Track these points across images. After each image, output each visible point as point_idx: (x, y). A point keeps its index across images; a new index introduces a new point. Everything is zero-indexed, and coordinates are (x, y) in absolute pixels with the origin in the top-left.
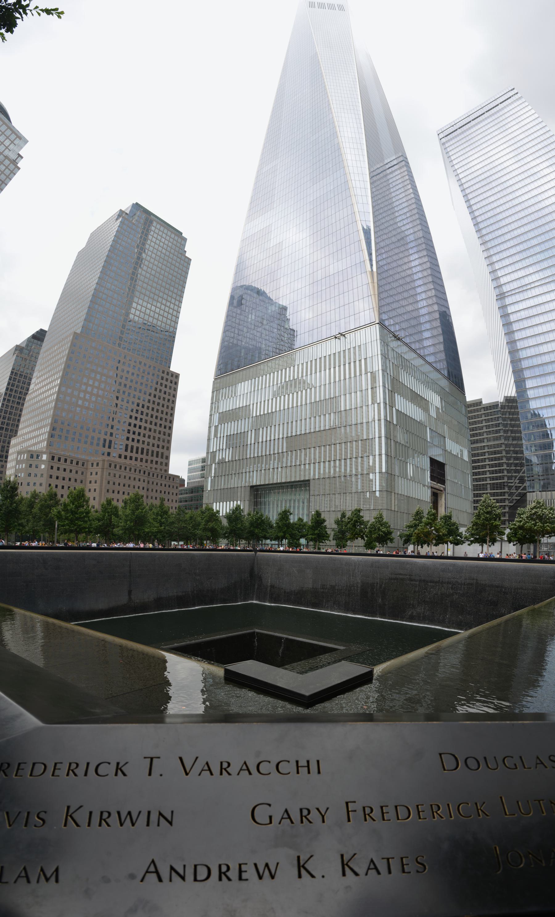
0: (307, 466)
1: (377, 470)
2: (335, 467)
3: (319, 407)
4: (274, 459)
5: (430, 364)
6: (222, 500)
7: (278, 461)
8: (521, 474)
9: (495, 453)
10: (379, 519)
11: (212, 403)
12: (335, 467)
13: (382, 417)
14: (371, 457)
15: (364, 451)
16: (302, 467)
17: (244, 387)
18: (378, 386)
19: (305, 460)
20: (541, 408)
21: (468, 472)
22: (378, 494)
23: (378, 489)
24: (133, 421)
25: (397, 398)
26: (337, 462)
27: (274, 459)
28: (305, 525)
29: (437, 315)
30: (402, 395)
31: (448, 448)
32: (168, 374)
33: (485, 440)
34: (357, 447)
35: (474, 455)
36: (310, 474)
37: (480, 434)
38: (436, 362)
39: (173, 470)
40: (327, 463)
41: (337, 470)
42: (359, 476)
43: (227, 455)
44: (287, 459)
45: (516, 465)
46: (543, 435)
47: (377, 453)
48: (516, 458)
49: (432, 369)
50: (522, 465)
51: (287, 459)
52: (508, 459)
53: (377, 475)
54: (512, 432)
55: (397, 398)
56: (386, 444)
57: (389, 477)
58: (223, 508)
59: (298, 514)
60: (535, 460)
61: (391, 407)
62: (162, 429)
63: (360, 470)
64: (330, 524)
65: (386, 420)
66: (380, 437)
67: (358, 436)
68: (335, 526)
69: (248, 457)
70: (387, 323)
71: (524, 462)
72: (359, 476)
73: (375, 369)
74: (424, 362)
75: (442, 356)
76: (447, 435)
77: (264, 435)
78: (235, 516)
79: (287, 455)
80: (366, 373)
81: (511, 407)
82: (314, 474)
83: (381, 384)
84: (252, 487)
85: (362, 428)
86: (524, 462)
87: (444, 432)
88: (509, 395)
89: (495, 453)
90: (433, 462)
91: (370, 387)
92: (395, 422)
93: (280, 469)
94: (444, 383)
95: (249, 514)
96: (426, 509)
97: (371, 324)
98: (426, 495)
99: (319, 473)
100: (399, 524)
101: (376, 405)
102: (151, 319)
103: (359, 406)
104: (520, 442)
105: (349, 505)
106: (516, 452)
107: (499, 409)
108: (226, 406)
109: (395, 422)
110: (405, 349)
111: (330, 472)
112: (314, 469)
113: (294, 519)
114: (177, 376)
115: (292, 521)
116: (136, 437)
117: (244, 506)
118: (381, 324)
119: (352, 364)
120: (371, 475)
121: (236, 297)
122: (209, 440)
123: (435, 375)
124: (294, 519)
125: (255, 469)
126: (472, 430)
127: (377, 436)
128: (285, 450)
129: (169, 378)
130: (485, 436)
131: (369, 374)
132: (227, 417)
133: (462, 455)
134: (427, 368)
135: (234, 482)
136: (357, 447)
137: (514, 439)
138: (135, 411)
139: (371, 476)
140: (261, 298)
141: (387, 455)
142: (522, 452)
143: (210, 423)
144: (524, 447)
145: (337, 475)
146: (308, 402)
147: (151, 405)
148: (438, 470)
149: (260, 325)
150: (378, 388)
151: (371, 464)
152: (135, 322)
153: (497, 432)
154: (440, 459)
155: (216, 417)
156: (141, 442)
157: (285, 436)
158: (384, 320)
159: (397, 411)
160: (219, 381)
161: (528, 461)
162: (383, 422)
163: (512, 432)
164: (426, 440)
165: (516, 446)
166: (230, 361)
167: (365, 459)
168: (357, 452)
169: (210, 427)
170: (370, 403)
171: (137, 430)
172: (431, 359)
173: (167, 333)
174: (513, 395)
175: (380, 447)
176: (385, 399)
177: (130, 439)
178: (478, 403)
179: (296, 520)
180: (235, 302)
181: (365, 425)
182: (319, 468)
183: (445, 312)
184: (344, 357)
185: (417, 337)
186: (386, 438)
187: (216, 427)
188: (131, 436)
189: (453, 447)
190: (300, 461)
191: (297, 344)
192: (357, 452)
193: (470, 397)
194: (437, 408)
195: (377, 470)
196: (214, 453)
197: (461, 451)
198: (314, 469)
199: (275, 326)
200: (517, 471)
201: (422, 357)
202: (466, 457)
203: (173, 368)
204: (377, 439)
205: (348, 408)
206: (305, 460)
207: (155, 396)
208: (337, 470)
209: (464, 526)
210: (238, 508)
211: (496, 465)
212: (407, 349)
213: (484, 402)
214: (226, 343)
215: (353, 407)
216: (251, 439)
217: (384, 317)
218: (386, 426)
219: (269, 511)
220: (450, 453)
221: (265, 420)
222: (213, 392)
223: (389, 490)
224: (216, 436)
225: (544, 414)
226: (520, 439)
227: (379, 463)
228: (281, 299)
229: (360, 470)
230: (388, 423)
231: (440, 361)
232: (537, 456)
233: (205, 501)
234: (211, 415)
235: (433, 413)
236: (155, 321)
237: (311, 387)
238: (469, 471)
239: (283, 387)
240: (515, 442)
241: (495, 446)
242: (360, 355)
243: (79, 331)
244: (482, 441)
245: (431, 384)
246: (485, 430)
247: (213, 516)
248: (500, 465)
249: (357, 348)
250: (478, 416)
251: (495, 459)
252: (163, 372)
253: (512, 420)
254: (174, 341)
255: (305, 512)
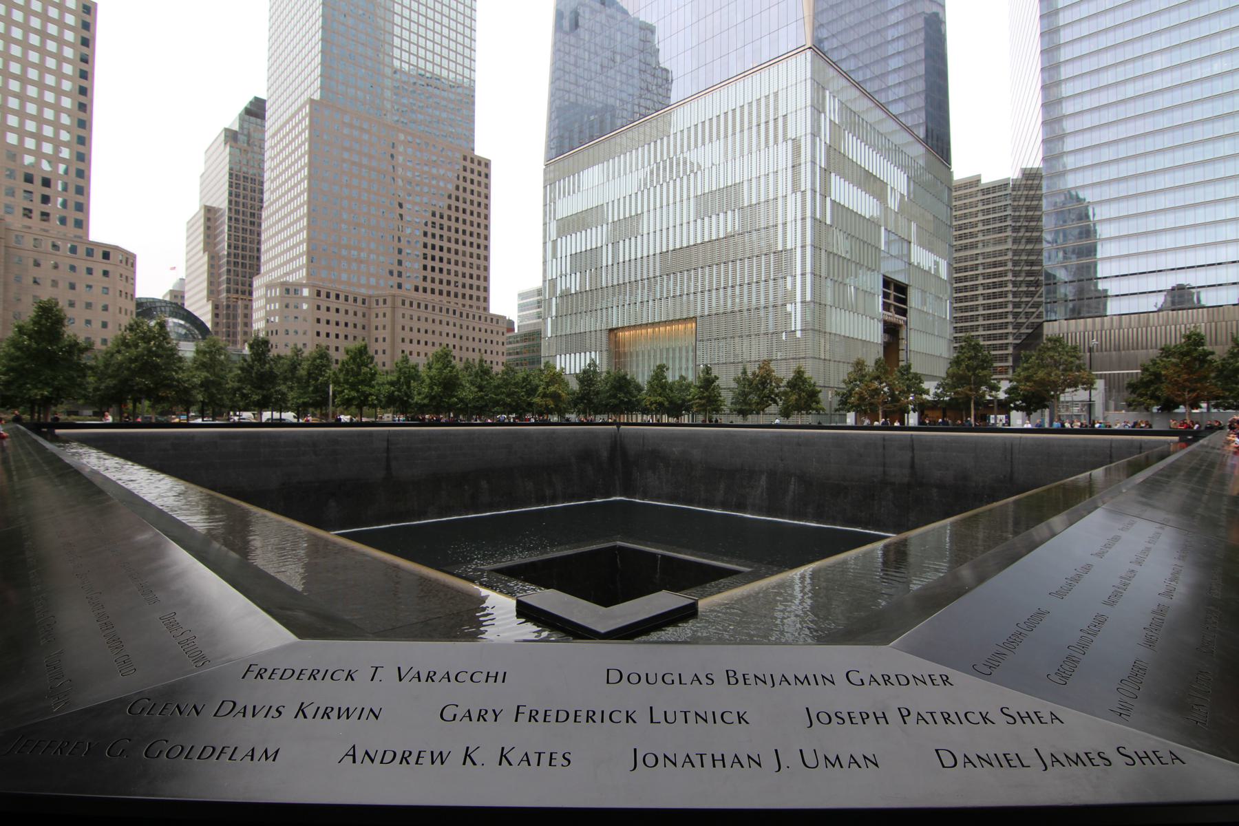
0: (692, 296)
1: (798, 299)
2: (733, 296)
3: (709, 204)
4: (643, 288)
5: (895, 118)
6: (568, 351)
7: (649, 291)
8: (1036, 299)
9: (995, 265)
10: (799, 374)
11: (545, 205)
12: (733, 296)
13: (808, 214)
14: (789, 279)
15: (778, 269)
16: (685, 297)
17: (592, 176)
18: (803, 161)
19: (688, 287)
20: (1083, 187)
21: (946, 297)
22: (798, 334)
23: (799, 327)
24: (430, 241)
25: (835, 180)
26: (737, 288)
27: (643, 288)
28: (689, 386)
29: (920, 23)
30: (843, 175)
31: (914, 259)
32: (472, 161)
33: (980, 245)
34: (768, 264)
35: (958, 270)
36: (696, 310)
37: (972, 235)
38: (905, 114)
39: (495, 308)
40: (721, 291)
41: (737, 300)
42: (771, 309)
43: (573, 284)
44: (662, 285)
45: (1029, 284)
46: (1081, 233)
47: (799, 272)
48: (1029, 273)
49: (898, 127)
50: (1037, 284)
51: (662, 285)
52: (1016, 274)
53: (799, 305)
54: (1028, 229)
55: (835, 180)
56: (813, 256)
57: (817, 306)
58: (571, 364)
59: (680, 368)
60: (1062, 275)
61: (824, 196)
62: (475, 250)
63: (771, 299)
64: (726, 381)
65: (814, 218)
66: (803, 247)
67: (769, 246)
68: (733, 385)
69: (604, 285)
70: (826, 46)
71: (1042, 278)
72: (771, 309)
73: (801, 132)
74: (884, 116)
75: (920, 102)
76: (913, 239)
77: (627, 251)
78: (587, 377)
79: (662, 280)
80: (785, 140)
81: (1031, 188)
82: (703, 308)
83: (809, 159)
84: (611, 330)
85: (776, 232)
86: (1042, 278)
87: (909, 235)
88: (1029, 166)
89: (995, 265)
90: (887, 282)
91: (790, 165)
92: (828, 222)
93: (651, 303)
94: (918, 151)
95: (608, 373)
96: (873, 356)
97: (798, 51)
98: (876, 334)
99: (710, 307)
100: (830, 379)
101: (799, 194)
102: (429, 67)
103: (771, 197)
104: (1037, 247)
105: (752, 353)
106: (1032, 263)
107: (1009, 191)
108: (568, 207)
109: (828, 222)
110: (855, 93)
111: (725, 304)
112: (703, 301)
113: (674, 376)
114: (487, 164)
115: (670, 380)
116: (437, 264)
117: (601, 359)
118: (817, 49)
119: (763, 126)
120: (789, 306)
121: (567, 14)
122: (545, 262)
123: (902, 138)
124: (674, 376)
125: (615, 304)
126: (960, 228)
127: (799, 244)
128: (658, 274)
129: (475, 166)
130: (980, 238)
131: (790, 142)
132: (569, 226)
133: (937, 270)
134: (891, 126)
135: (586, 324)
136: (768, 264)
137: (1029, 241)
138: (430, 224)
139: (789, 307)
140: (609, 11)
141: (813, 274)
142: (1039, 263)
143: (545, 237)
144: (1045, 254)
145: (736, 309)
146: (692, 195)
147: (454, 214)
148: (896, 292)
149: (611, 64)
150: (803, 166)
151: (789, 287)
152: (404, 73)
153: (1001, 230)
154: (901, 278)
155: (553, 227)
156: (445, 271)
157: (658, 251)
158: (821, 41)
159: (833, 202)
160: (552, 168)
161: (1049, 276)
162: (809, 221)
163: (1028, 229)
164: (878, 249)
165: (1030, 253)
166: (567, 134)
167: (780, 282)
168: (768, 273)
169: (545, 243)
170: (789, 191)
171: (437, 253)
172: (896, 109)
173: (460, 90)
174: (1036, 166)
175: (802, 263)
176: (813, 183)
177: (429, 268)
178: (976, 181)
179: (677, 378)
180: (566, 24)
181: (780, 227)
182: (710, 300)
183: (936, 15)
184: (750, 114)
185: (877, 70)
186: (814, 246)
187: (555, 242)
188: (430, 263)
189: (922, 257)
190: (682, 289)
191: (675, 96)
192: (768, 273)
193: (961, 169)
194: (902, 195)
195: (798, 299)
196: (553, 282)
197: (936, 263)
198: (703, 301)
199: (636, 65)
200: (1027, 294)
201: (882, 107)
202: (944, 274)
203: (480, 151)
204: (799, 250)
205: (754, 202)
206: (688, 287)
207: (457, 199)
208: (737, 300)
209: (933, 378)
210: (593, 363)
211: (995, 285)
212: (858, 93)
213: (985, 180)
214: (558, 102)
215: (762, 200)
216: (606, 258)
217: (824, 33)
218: (813, 227)
219: (637, 366)
220: (918, 267)
221: (627, 227)
222: (545, 187)
223: (817, 327)
224: (554, 256)
225: (1088, 195)
226: (1039, 240)
227: (799, 286)
228: (642, 12)
229: (771, 299)
230: (818, 223)
231: (913, 111)
232: (1066, 267)
233: (544, 352)
234: (545, 224)
235: (893, 204)
236: (437, 70)
237: (696, 169)
238: (947, 294)
239: (652, 173)
240: (1029, 247)
241: (995, 254)
242: (776, 109)
243: (317, 96)
244: (973, 246)
245: (893, 153)
246: (980, 227)
247: (557, 378)
248: (1001, 284)
249: (772, 97)
250: (971, 205)
251: (995, 275)
252: (465, 159)
253: (1028, 208)
254: (473, 103)
255: (691, 365)
